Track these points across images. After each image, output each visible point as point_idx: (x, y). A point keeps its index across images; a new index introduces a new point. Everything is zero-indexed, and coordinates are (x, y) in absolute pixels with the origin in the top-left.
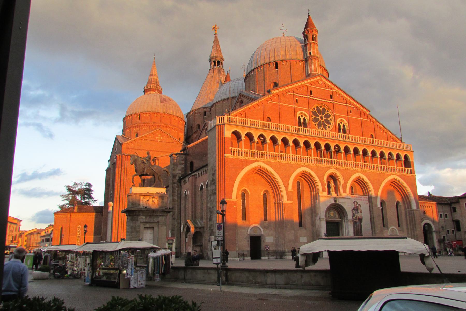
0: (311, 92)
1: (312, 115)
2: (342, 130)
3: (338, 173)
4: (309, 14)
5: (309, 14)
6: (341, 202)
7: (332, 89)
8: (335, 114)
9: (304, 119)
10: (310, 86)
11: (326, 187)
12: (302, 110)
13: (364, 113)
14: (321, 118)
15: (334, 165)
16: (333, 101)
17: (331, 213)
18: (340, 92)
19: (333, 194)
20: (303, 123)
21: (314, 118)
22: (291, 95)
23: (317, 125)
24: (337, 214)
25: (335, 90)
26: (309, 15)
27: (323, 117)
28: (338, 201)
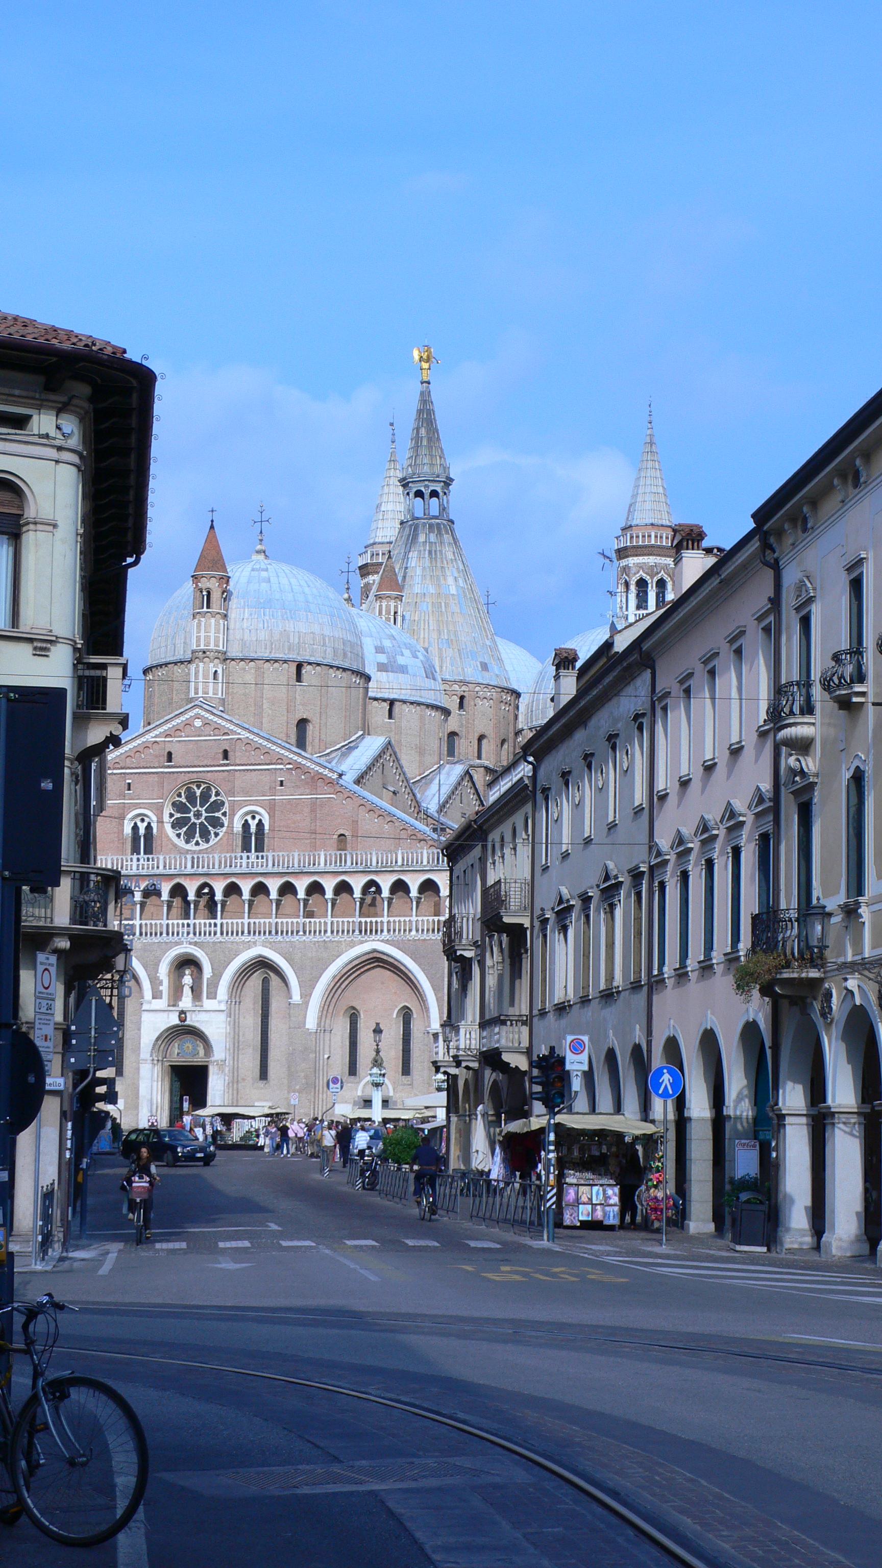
0: (170, 755)
1: (173, 812)
2: (253, 838)
3: (199, 954)
4: (212, 521)
5: (212, 521)
6: (198, 1021)
7: (229, 735)
8: (229, 799)
9: (149, 828)
10: (167, 739)
11: (165, 988)
12: (140, 808)
13: (322, 777)
14: (198, 815)
15: (191, 935)
16: (227, 765)
17: (187, 1045)
18: (252, 737)
19: (186, 1002)
20: (145, 836)
21: (177, 818)
22: (115, 774)
23: (182, 836)
24: (202, 1047)
25: (239, 734)
26: (212, 527)
27: (204, 812)
28: (188, 1019)
